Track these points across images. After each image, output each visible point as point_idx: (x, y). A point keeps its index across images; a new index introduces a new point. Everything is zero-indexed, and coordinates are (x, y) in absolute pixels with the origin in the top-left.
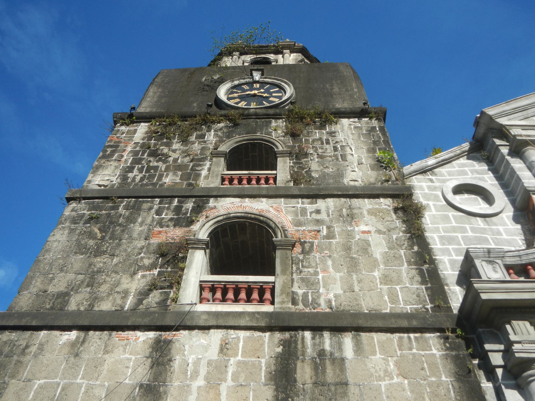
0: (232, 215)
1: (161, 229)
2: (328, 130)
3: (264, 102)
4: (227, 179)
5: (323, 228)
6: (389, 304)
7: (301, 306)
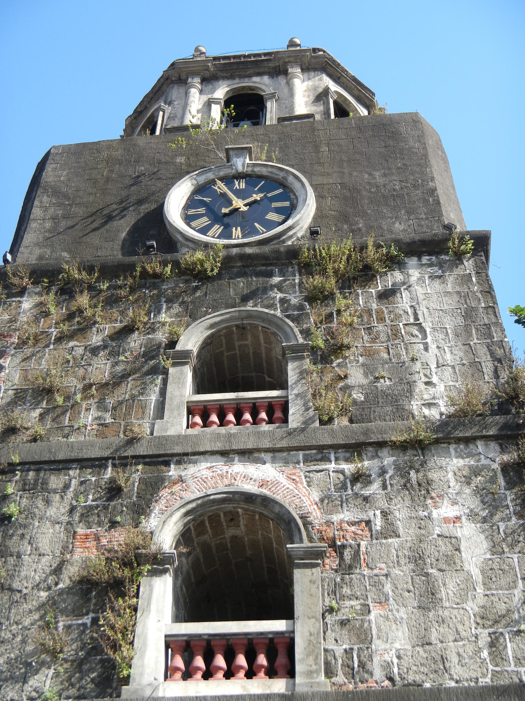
0: (212, 497)
1: (89, 531)
2: (380, 288)
3: (256, 224)
4: (198, 411)
5: (374, 515)
6: (491, 667)
7: (340, 678)
